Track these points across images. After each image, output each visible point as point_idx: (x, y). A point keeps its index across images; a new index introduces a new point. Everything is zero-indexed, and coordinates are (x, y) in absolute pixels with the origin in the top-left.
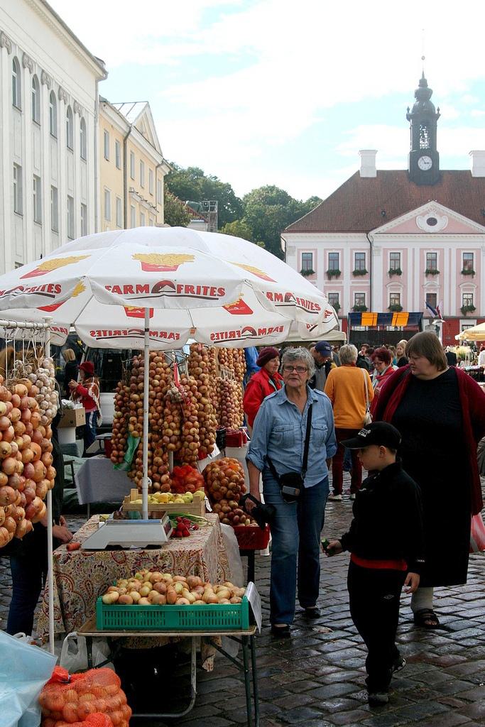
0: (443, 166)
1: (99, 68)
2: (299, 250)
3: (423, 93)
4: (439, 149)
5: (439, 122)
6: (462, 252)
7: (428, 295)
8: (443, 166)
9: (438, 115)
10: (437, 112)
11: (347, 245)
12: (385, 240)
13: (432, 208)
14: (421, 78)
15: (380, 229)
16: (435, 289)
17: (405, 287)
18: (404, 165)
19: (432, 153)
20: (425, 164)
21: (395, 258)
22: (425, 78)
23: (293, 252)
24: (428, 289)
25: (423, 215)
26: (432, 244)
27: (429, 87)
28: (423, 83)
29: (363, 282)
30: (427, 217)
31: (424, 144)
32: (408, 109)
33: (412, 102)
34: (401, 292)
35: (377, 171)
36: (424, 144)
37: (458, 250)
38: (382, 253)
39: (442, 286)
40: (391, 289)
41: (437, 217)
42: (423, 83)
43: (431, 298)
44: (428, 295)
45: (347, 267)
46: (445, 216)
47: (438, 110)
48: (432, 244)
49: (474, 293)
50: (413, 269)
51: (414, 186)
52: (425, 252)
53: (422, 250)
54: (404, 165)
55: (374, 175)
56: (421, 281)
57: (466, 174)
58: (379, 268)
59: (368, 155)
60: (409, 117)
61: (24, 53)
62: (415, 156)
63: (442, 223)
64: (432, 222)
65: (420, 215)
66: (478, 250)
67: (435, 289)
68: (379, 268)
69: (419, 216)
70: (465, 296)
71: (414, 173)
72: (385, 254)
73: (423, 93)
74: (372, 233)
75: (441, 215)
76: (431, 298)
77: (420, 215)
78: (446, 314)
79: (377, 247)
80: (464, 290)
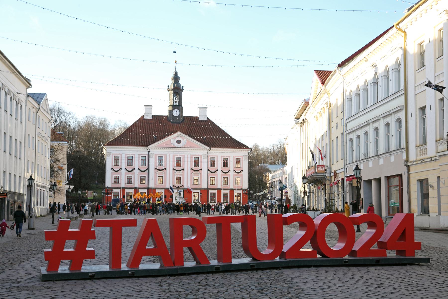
0: (185, 114)
1: (27, 82)
2: (113, 154)
3: (176, 78)
4: (183, 104)
5: (183, 93)
6: (194, 157)
9: (183, 89)
10: (182, 88)
13: (179, 135)
14: (175, 70)
18: (166, 114)
20: (176, 113)
21: (161, 160)
22: (177, 71)
23: (110, 155)
24: (177, 175)
25: (175, 138)
28: (176, 74)
30: (176, 140)
32: (168, 86)
33: (170, 83)
34: (163, 176)
35: (153, 116)
37: (191, 156)
38: (154, 156)
40: (158, 175)
41: (181, 140)
42: (176, 74)
45: (137, 164)
46: (185, 139)
47: (183, 87)
49: (199, 176)
50: (170, 164)
52: (175, 157)
55: (151, 118)
57: (197, 118)
58: (153, 163)
59: (148, 107)
61: (3, 84)
63: (183, 142)
64: (179, 142)
65: (174, 138)
66: (201, 156)
68: (153, 163)
69: (173, 138)
70: (195, 178)
72: (156, 158)
73: (176, 78)
74: (149, 147)
77: (174, 138)
78: (185, 186)
79: (152, 153)
80: (194, 175)
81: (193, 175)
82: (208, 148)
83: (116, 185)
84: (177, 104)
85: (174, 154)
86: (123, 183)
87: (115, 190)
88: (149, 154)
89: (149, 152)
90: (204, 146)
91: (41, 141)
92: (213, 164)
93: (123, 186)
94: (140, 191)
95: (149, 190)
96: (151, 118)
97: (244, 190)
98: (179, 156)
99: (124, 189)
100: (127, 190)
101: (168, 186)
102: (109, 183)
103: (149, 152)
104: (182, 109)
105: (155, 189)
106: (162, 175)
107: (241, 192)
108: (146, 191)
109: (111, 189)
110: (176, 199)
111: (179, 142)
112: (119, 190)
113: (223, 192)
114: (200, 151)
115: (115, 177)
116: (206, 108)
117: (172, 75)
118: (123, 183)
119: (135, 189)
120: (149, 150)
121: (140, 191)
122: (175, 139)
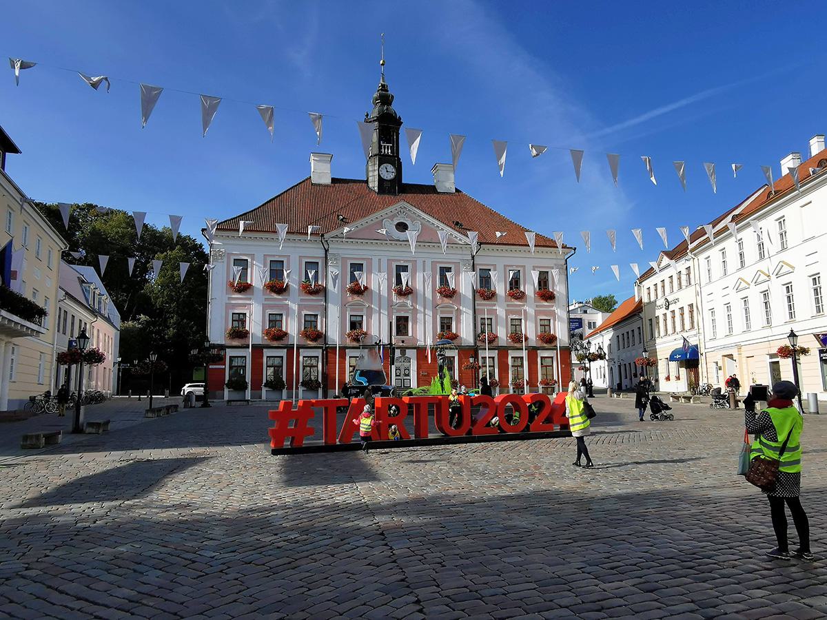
3: (385, 99)
6: (439, 266)
7: (399, 319)
16: (407, 311)
24: (398, 311)
25: (392, 218)
67: (407, 311)
73: (385, 99)
80: (442, 312)
81: (439, 311)
85: (390, 258)
87: (230, 353)
88: (326, 257)
89: (326, 251)
98: (402, 263)
102: (217, 332)
103: (326, 251)
106: (362, 310)
109: (222, 347)
110: (396, 376)
114: (454, 252)
115: (236, 317)
120: (326, 247)
122: (392, 220)
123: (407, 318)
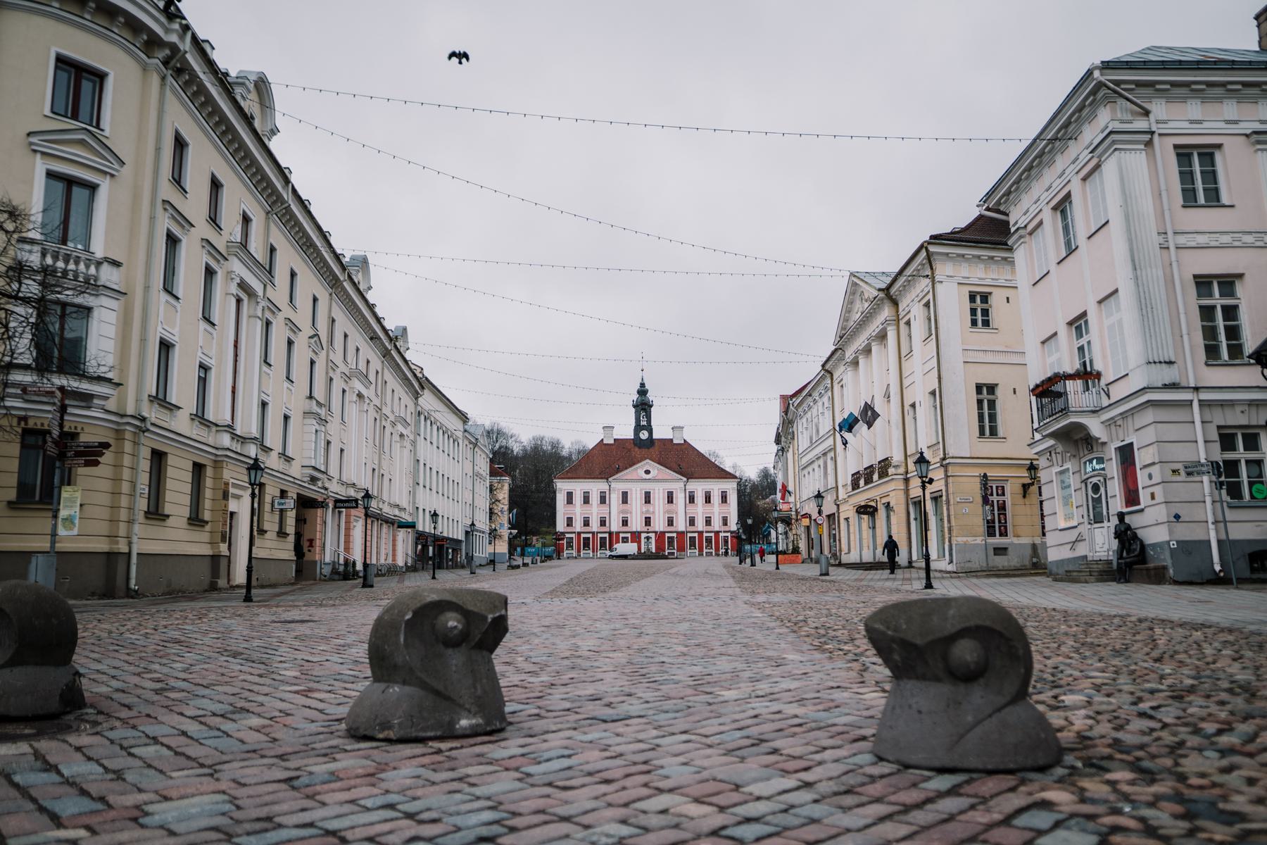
0: (655, 436)
1: (463, 417)
3: (642, 392)
4: (653, 423)
7: (646, 518)
8: (655, 436)
9: (651, 406)
11: (595, 487)
12: (617, 486)
13: (648, 464)
15: (614, 477)
17: (631, 513)
18: (630, 435)
19: (649, 429)
20: (644, 435)
21: (625, 495)
26: (648, 487)
27: (647, 387)
28: (642, 385)
29: (604, 511)
31: (644, 423)
33: (635, 397)
36: (644, 423)
39: (654, 512)
42: (642, 385)
43: (648, 521)
44: (646, 518)
46: (656, 470)
48: (648, 487)
51: (637, 449)
53: (641, 490)
54: (630, 435)
55: (612, 442)
56: (641, 509)
57: (672, 440)
58: (615, 499)
60: (634, 406)
62: (638, 428)
63: (653, 473)
64: (647, 472)
67: (650, 514)
69: (638, 470)
71: (637, 442)
73: (642, 392)
75: (654, 469)
76: (648, 521)
78: (657, 529)
82: (685, 479)
83: (569, 529)
84: (645, 423)
86: (578, 526)
87: (567, 535)
90: (680, 477)
91: (479, 480)
92: (692, 499)
93: (578, 529)
94: (600, 535)
95: (610, 534)
96: (612, 442)
97: (732, 532)
99: (579, 534)
100: (583, 535)
101: (634, 530)
102: (561, 526)
104: (651, 430)
105: (618, 533)
107: (729, 534)
108: (607, 535)
109: (563, 533)
111: (647, 472)
112: (573, 535)
113: (705, 535)
116: (683, 427)
117: (638, 387)
118: (578, 526)
119: (593, 533)
121: (600, 535)
123: (650, 518)
